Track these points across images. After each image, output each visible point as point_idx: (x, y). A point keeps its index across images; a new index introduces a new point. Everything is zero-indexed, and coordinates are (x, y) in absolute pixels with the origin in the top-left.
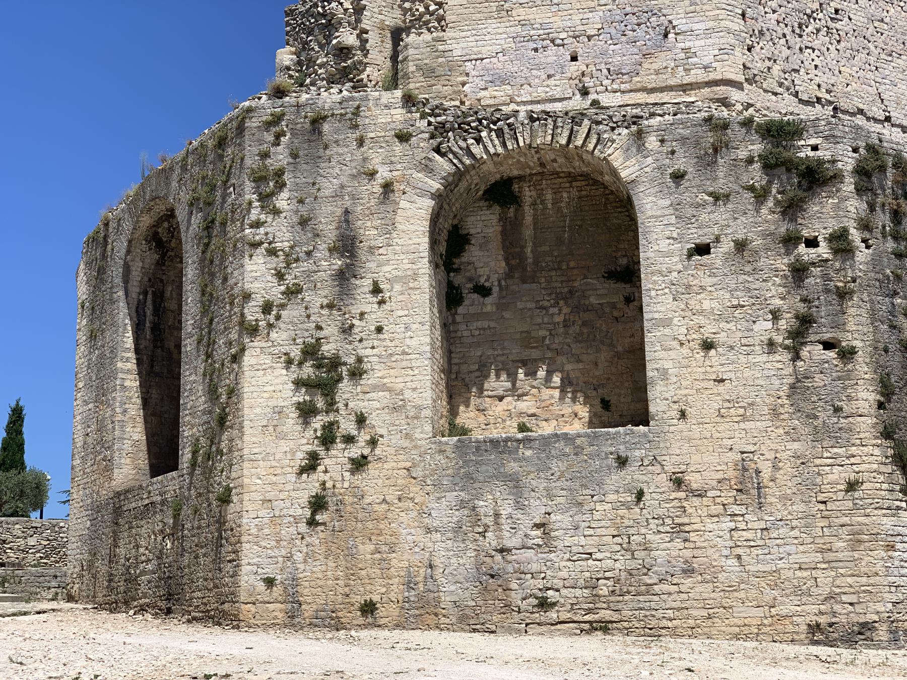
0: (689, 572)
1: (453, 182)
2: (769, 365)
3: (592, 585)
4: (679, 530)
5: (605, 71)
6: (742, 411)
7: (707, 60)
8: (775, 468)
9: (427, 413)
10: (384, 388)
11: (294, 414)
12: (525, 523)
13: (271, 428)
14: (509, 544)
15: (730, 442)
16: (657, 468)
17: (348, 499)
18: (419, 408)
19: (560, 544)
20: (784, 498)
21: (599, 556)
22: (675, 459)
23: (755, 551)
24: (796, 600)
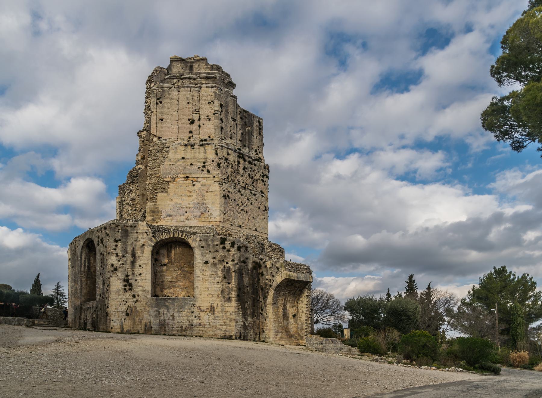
0: (200, 325)
1: (157, 243)
3: (182, 327)
4: (199, 318)
8: (217, 306)
9: (150, 292)
10: (141, 286)
11: (122, 292)
12: (169, 315)
17: (133, 309)
18: (148, 291)
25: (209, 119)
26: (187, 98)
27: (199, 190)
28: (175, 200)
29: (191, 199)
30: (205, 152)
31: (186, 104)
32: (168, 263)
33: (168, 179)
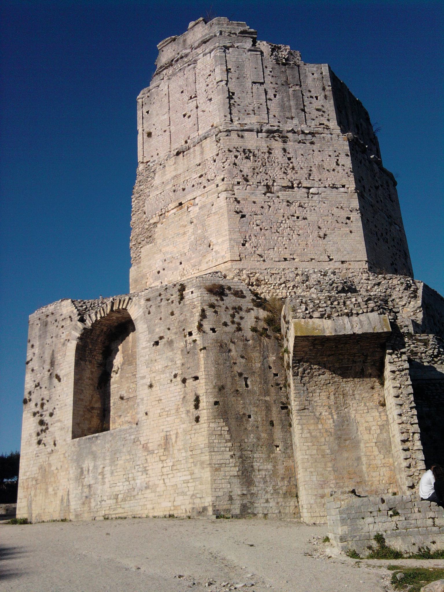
0: (147, 488)
2: (176, 391)
4: (145, 471)
5: (191, 266)
6: (166, 413)
7: (224, 253)
9: (71, 429)
13: (28, 443)
14: (92, 482)
15: (162, 427)
16: (138, 443)
19: (106, 480)
20: (179, 450)
21: (118, 484)
22: (145, 439)
23: (170, 476)
24: (181, 498)
25: (210, 100)
26: (180, 86)
27: (197, 217)
28: (164, 250)
29: (186, 237)
30: (202, 153)
31: (178, 95)
32: (123, 364)
33: (155, 220)
